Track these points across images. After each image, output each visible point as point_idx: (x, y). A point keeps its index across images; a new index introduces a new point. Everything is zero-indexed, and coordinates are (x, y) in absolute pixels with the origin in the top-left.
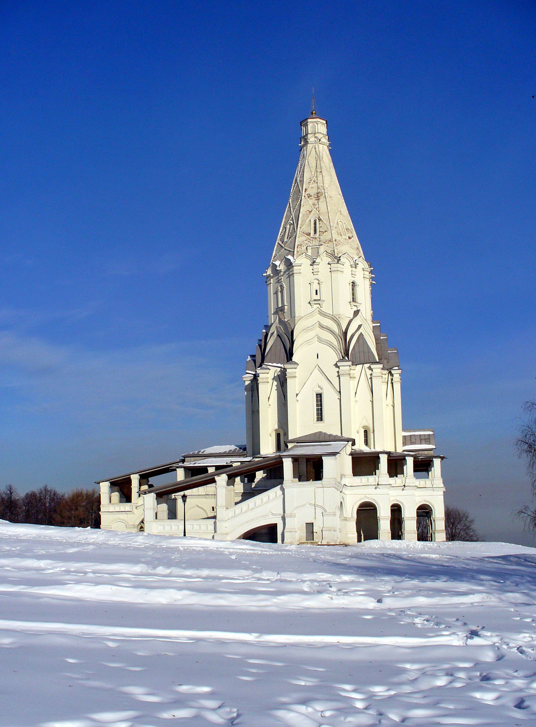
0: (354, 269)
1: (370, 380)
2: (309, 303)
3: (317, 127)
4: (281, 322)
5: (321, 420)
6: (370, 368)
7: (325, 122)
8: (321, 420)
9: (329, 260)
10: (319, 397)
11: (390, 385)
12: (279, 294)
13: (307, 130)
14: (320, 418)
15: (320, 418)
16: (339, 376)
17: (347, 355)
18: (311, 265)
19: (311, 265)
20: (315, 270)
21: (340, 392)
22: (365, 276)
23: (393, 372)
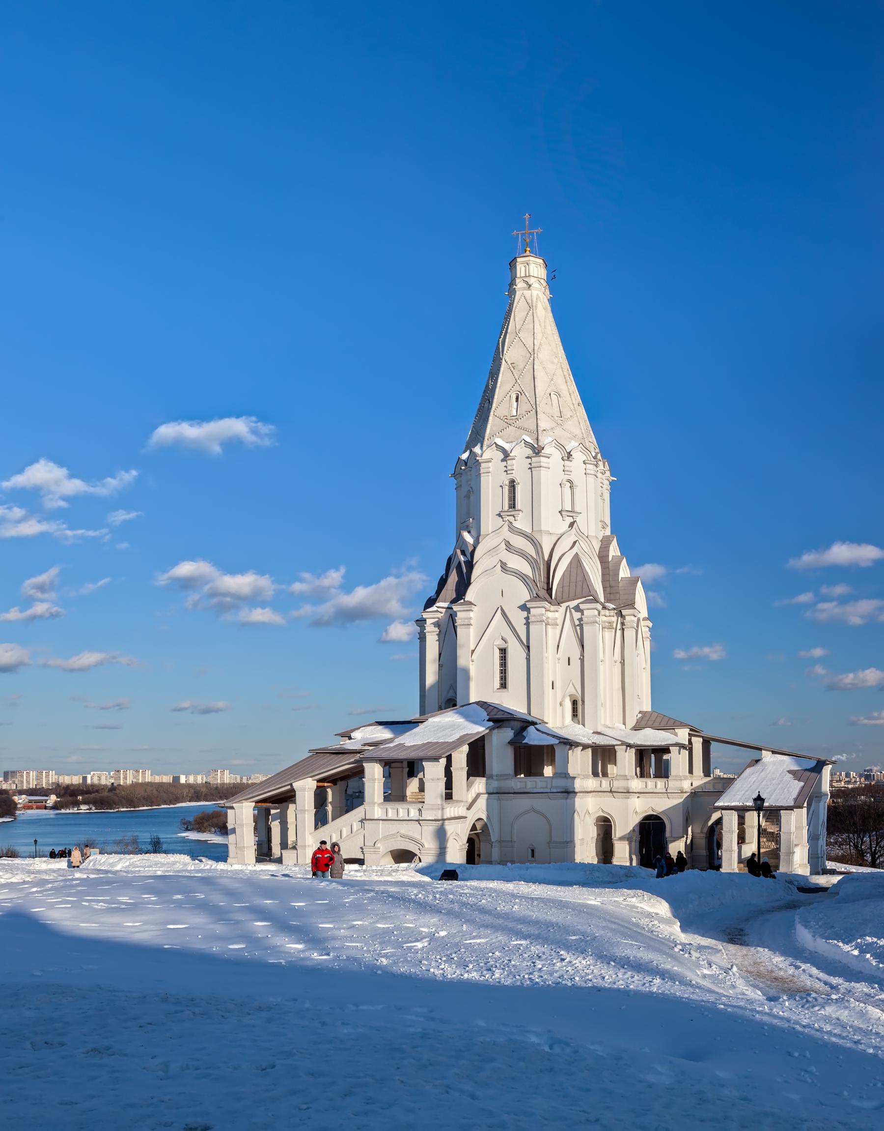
0: (567, 463)
2: (499, 515)
3: (532, 270)
5: (505, 687)
7: (541, 261)
8: (505, 687)
9: (529, 452)
10: (503, 651)
11: (619, 633)
14: (504, 685)
15: (504, 685)
17: (549, 590)
18: (503, 460)
19: (503, 460)
20: (509, 468)
21: (528, 647)
22: (588, 471)
23: (624, 612)
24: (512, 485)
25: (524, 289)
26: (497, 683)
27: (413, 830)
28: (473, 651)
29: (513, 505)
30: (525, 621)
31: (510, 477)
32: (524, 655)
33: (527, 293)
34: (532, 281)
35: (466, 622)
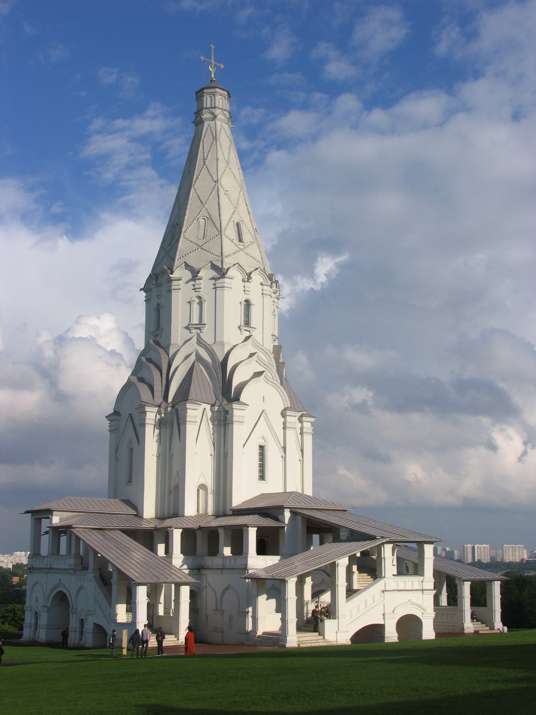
1: (299, 436)
4: (200, 342)
6: (300, 420)
10: (262, 448)
12: (196, 307)
13: (213, 101)
14: (262, 477)
15: (262, 477)
16: (285, 428)
20: (246, 289)
24: (248, 304)
25: (222, 120)
26: (257, 474)
27: (417, 597)
28: (244, 445)
29: (247, 323)
30: (282, 426)
31: (246, 297)
32: (280, 453)
33: (212, 123)
34: (217, 112)
35: (241, 420)
